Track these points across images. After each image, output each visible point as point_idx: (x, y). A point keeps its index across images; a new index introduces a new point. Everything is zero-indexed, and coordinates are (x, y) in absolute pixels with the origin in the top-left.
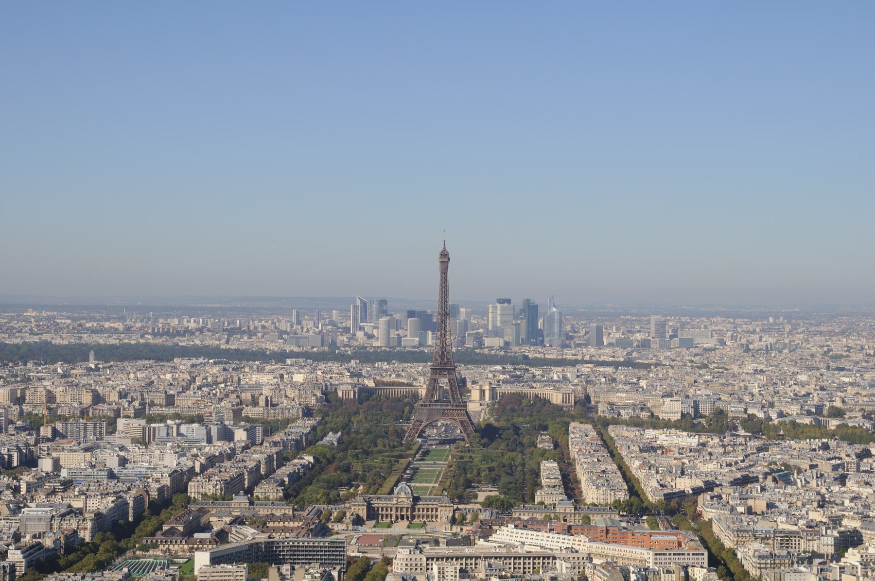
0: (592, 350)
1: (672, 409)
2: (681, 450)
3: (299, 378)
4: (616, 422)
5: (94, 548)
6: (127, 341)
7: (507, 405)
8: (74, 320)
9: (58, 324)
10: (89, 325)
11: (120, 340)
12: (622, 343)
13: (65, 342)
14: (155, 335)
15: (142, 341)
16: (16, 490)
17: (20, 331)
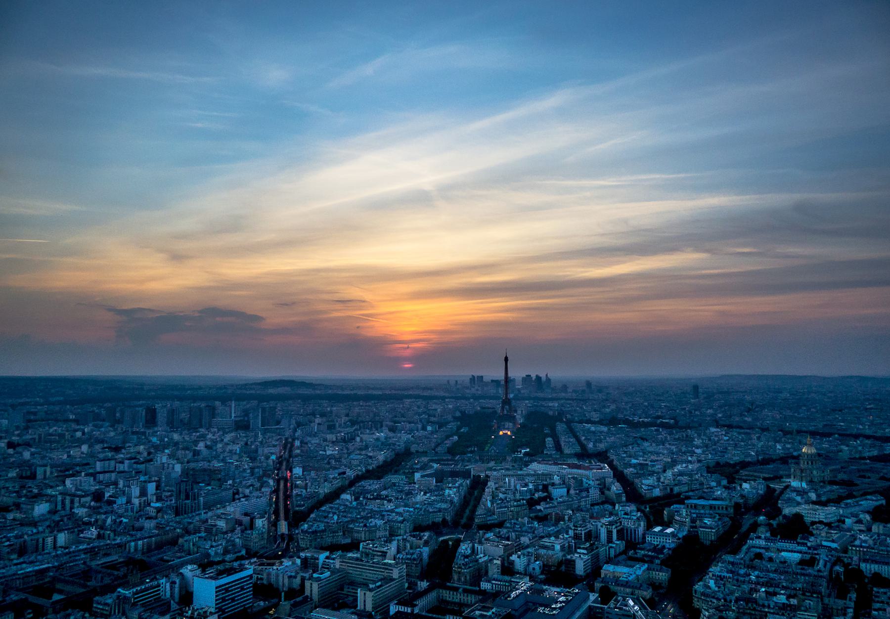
0: (563, 394)
1: (595, 416)
2: (601, 432)
3: (451, 406)
4: (573, 422)
7: (531, 416)
12: (574, 391)
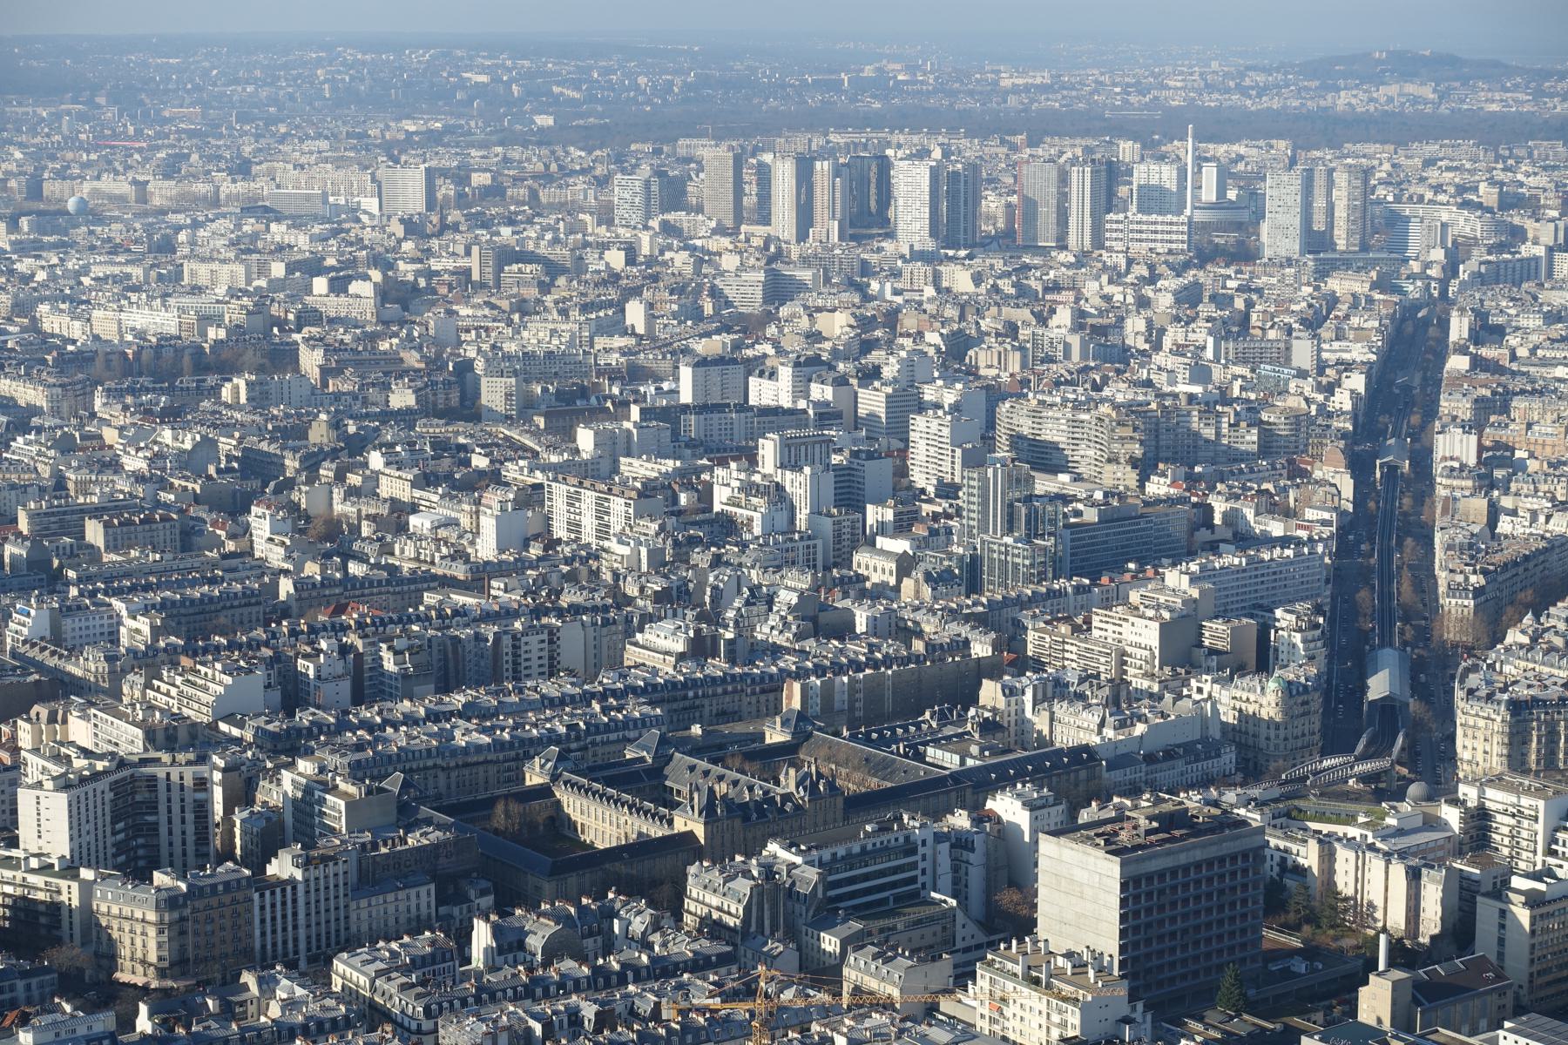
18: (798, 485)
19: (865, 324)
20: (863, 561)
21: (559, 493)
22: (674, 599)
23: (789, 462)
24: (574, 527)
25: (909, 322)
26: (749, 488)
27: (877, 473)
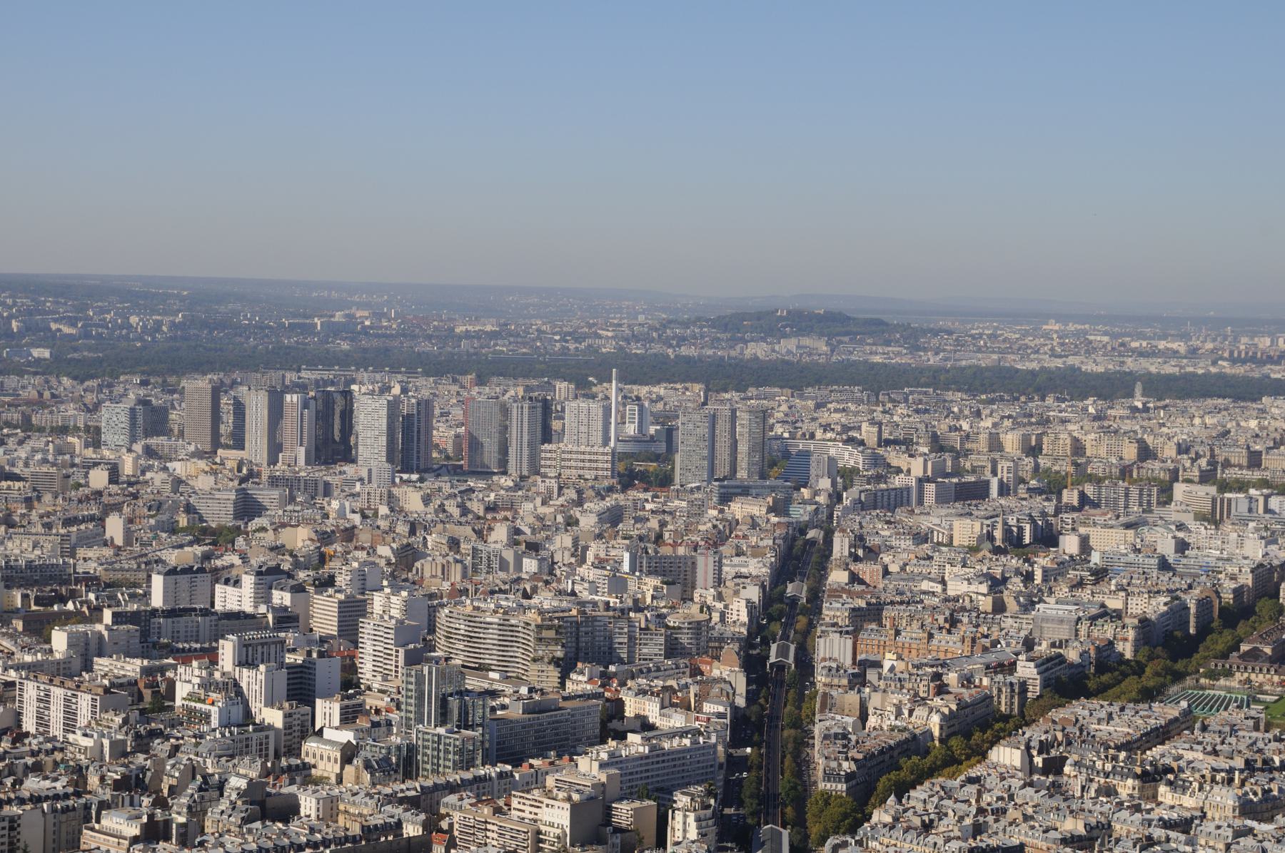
5: (1137, 669)
6: (1190, 369)
8: (1114, 336)
9: (1091, 342)
10: (1135, 345)
11: (1181, 367)
13: (1101, 369)
14: (1234, 361)
15: (1213, 370)
16: (1029, 577)
17: (1037, 352)
18: (253, 681)
19: (325, 538)
20: (310, 746)
21: (31, 691)
22: (131, 785)
23: (246, 661)
24: (42, 721)
25: (364, 538)
26: (207, 685)
27: (328, 671)
